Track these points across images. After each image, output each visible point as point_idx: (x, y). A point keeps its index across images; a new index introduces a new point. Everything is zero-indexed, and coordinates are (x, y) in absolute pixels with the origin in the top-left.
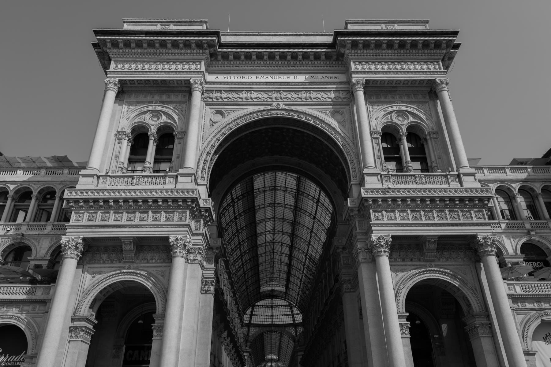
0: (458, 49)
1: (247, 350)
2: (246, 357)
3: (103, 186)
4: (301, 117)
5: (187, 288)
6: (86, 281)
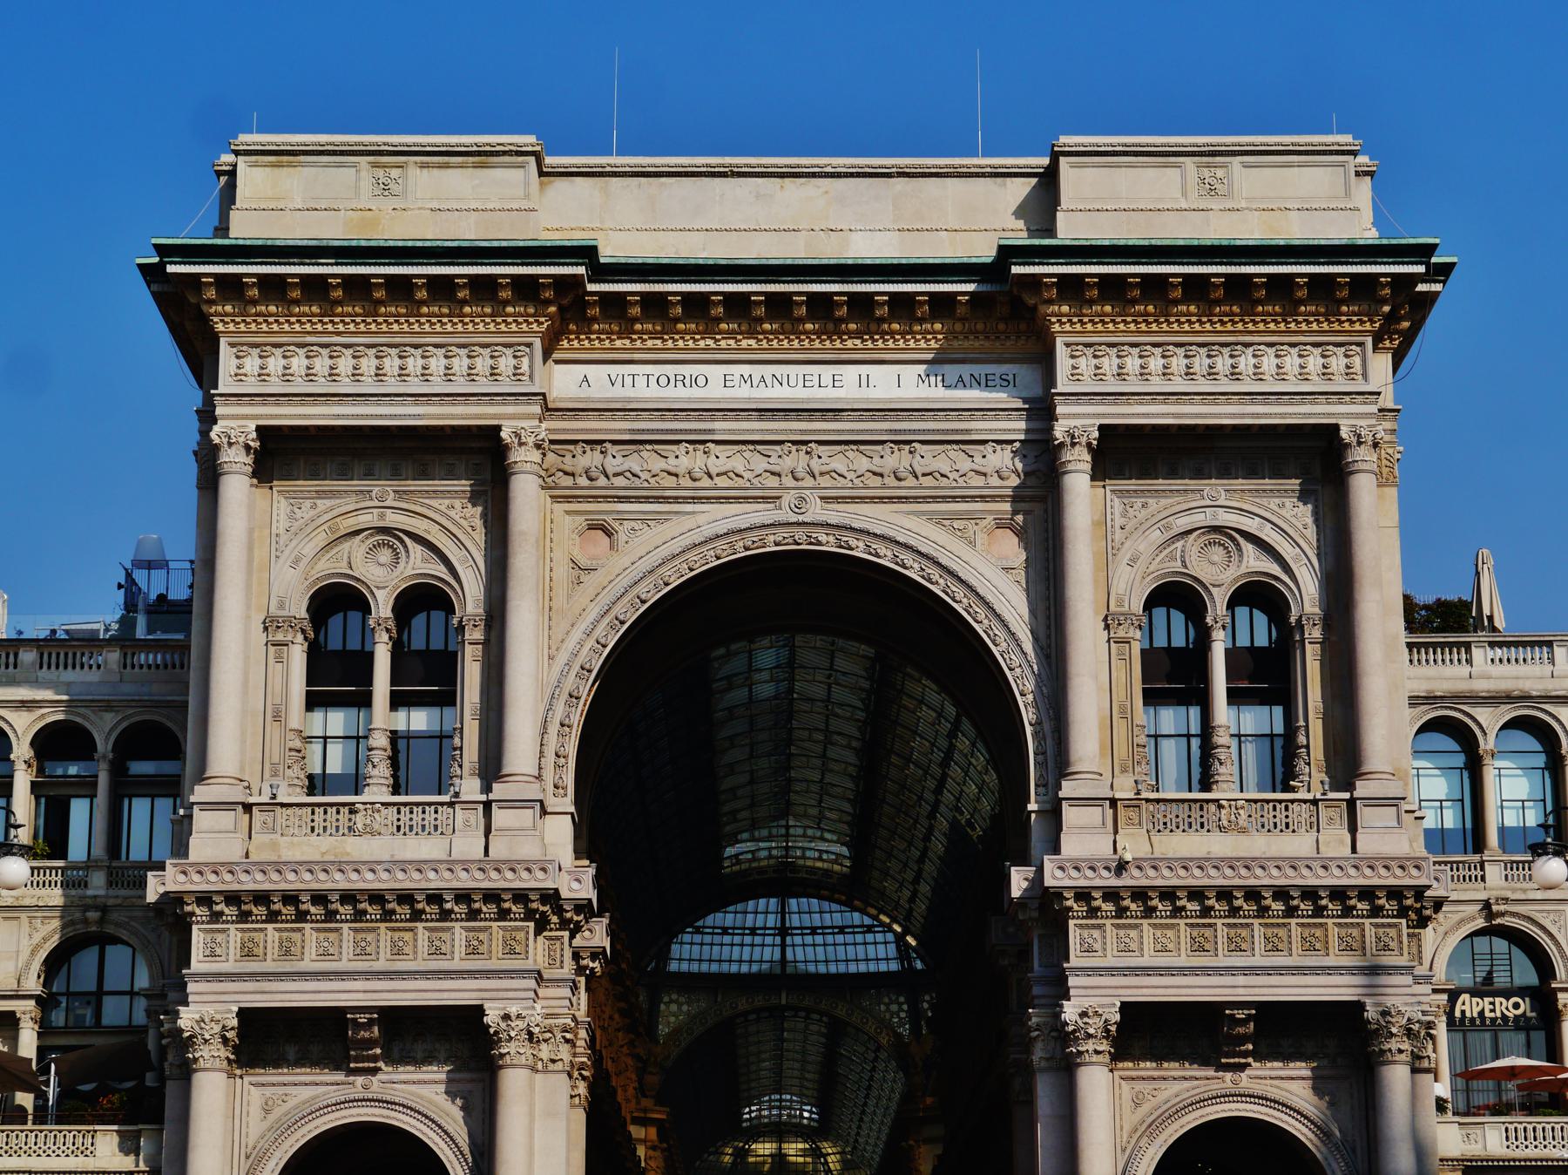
0: (1444, 282)
1: (645, 1111)
2: (641, 1151)
3: (266, 838)
4: (877, 556)
5: (536, 1147)
6: (250, 1125)
